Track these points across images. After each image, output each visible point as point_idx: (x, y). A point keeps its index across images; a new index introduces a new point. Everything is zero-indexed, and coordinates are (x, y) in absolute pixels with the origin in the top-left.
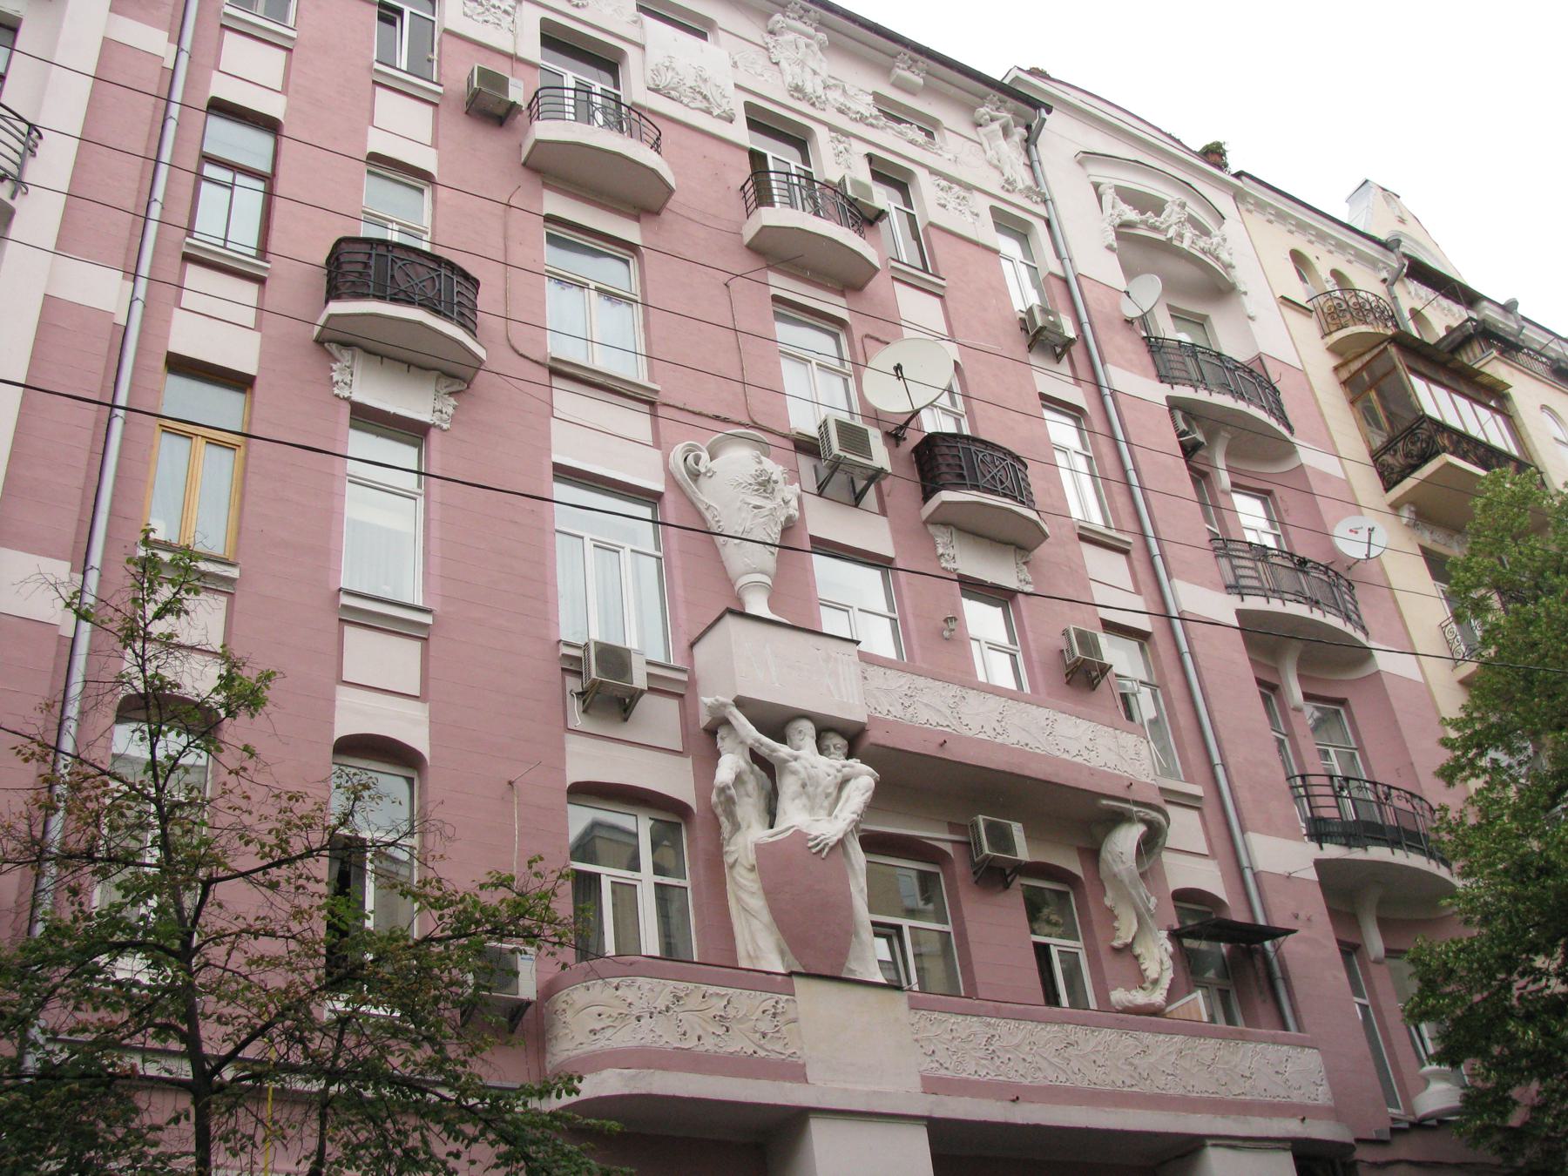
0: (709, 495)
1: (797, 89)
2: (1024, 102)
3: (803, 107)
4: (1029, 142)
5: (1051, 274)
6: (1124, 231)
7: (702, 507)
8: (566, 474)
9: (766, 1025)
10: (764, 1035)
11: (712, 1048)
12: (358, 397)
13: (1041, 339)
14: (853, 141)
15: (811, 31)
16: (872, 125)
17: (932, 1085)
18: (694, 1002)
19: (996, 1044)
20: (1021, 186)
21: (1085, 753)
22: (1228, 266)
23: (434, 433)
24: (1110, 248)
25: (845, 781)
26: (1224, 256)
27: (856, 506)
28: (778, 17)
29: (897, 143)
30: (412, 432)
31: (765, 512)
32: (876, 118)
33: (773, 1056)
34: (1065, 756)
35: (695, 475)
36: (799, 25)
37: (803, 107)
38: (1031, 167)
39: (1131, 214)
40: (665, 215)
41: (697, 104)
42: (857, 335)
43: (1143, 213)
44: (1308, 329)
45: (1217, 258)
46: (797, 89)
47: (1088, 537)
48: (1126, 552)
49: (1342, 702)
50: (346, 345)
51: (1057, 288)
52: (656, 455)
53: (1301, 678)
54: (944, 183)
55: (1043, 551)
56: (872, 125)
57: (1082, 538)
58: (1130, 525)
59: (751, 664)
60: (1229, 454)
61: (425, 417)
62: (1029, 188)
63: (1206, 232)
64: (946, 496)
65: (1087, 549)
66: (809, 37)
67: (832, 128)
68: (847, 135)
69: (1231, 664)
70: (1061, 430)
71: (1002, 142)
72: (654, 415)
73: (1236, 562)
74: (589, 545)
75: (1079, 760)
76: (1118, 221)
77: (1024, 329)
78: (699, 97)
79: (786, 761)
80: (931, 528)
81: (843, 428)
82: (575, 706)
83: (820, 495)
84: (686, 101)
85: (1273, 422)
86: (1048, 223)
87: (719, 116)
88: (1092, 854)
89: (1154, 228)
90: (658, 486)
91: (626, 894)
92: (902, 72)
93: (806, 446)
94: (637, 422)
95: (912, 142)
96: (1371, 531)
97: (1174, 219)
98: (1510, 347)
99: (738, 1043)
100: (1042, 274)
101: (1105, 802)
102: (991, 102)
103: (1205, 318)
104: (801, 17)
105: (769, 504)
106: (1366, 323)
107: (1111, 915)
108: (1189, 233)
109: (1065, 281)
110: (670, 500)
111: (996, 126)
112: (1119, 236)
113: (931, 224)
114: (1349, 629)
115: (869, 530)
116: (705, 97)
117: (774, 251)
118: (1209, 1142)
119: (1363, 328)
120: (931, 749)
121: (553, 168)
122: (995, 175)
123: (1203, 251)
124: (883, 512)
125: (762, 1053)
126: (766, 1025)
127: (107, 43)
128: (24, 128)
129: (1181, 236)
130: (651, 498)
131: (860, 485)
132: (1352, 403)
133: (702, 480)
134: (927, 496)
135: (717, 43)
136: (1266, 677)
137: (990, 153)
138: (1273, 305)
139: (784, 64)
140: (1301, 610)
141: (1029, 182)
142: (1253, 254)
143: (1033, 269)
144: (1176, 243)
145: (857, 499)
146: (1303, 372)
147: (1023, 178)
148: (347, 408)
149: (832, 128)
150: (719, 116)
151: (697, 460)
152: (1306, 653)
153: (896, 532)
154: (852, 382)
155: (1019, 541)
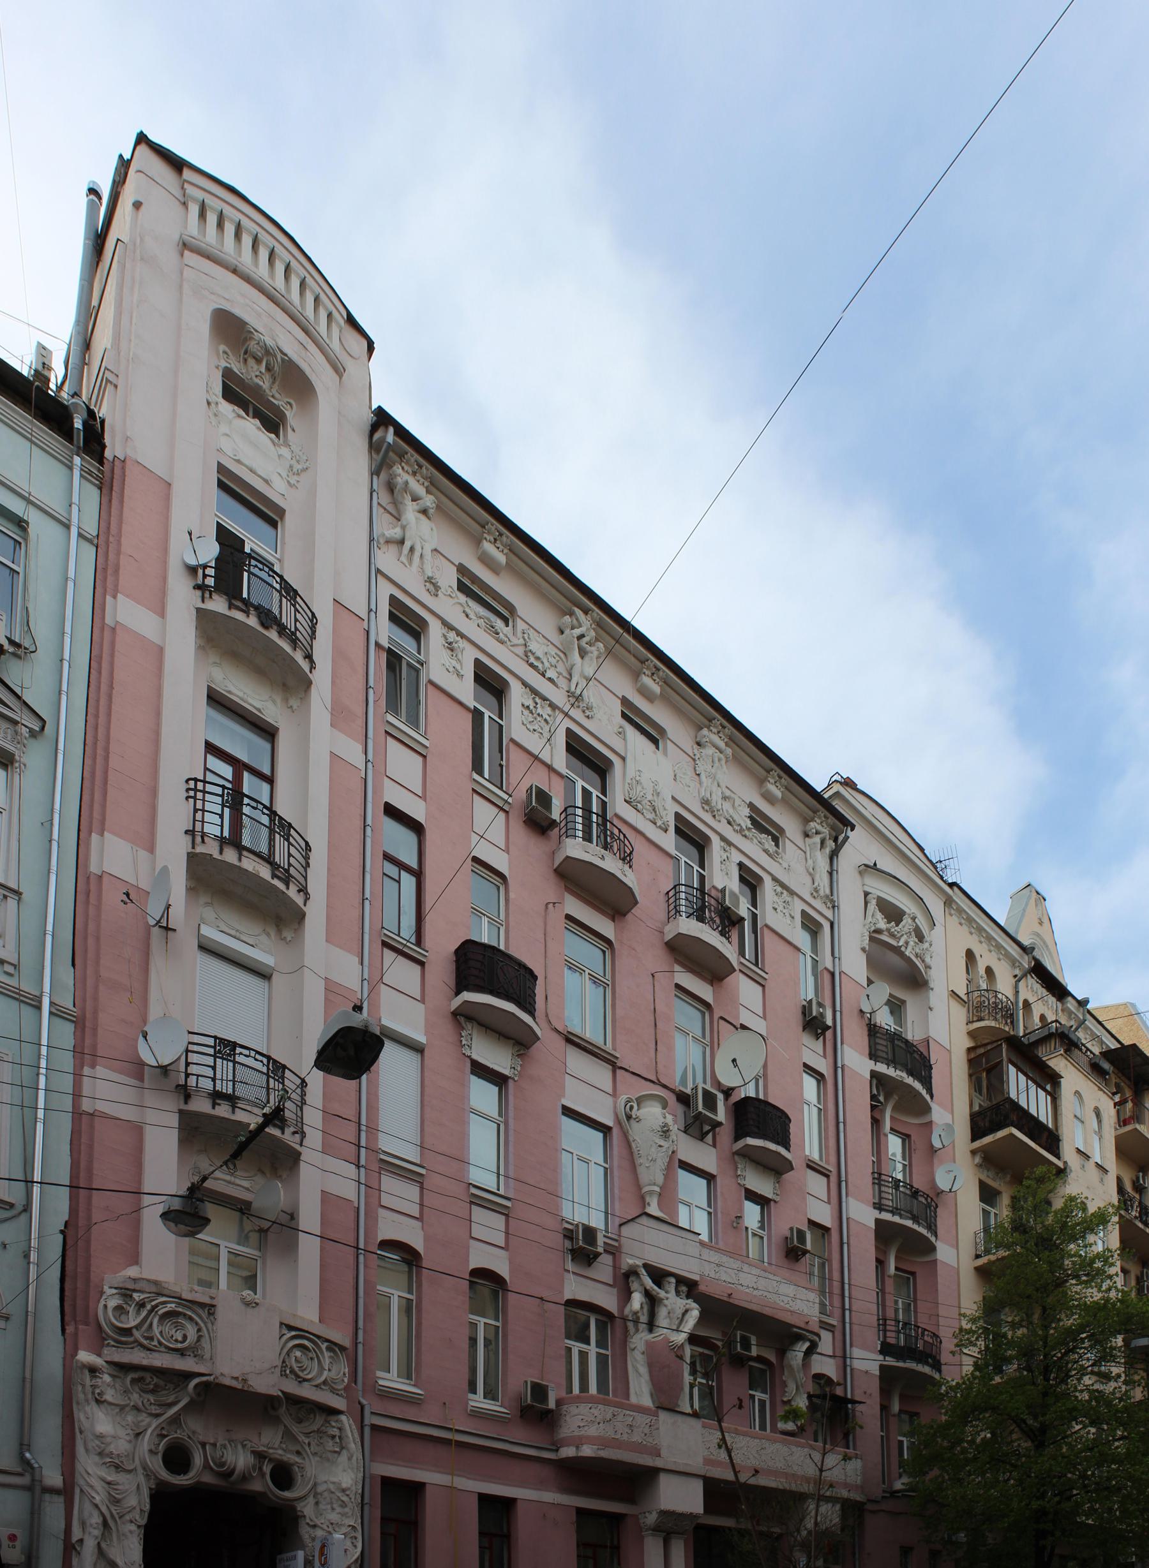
0: (637, 1132)
2: (831, 812)
4: (834, 855)
5: (826, 969)
6: (874, 936)
7: (631, 1139)
8: (568, 1112)
13: (814, 1025)
14: (733, 850)
20: (822, 893)
22: (928, 967)
23: (510, 1081)
24: (863, 950)
26: (928, 960)
32: (749, 829)
35: (629, 1117)
38: (831, 874)
39: (882, 924)
40: (629, 916)
42: (716, 1017)
43: (889, 922)
44: (960, 1014)
45: (923, 961)
46: (706, 802)
47: (811, 1166)
48: (827, 1176)
49: (913, 1274)
51: (827, 977)
52: (610, 1100)
53: (896, 1258)
54: (779, 889)
55: (788, 1176)
56: (745, 836)
57: (809, 1166)
58: (833, 1159)
59: (647, 1245)
61: (506, 1072)
62: (827, 896)
63: (921, 938)
64: (751, 1141)
65: (809, 1171)
67: (723, 839)
68: (730, 844)
69: (864, 1250)
70: (809, 1085)
71: (818, 853)
72: (614, 1072)
73: (883, 1189)
74: (575, 1158)
77: (804, 1013)
80: (736, 1157)
81: (706, 1093)
83: (685, 1132)
85: (924, 1092)
86: (832, 924)
89: (892, 935)
90: (609, 1122)
93: (684, 1099)
94: (601, 1075)
96: (958, 1175)
97: (906, 930)
98: (1068, 1042)
100: (820, 968)
103: (903, 1002)
106: (995, 1019)
108: (913, 940)
109: (833, 974)
110: (616, 1132)
112: (871, 939)
113: (767, 926)
114: (929, 1235)
115: (705, 1156)
119: (993, 1024)
122: (808, 880)
124: (714, 1145)
129: (907, 943)
130: (605, 1130)
131: (707, 1128)
132: (970, 1076)
133: (632, 1121)
134: (737, 1138)
135: (665, 753)
136: (881, 1258)
137: (810, 862)
138: (946, 994)
140: (909, 1223)
141: (828, 892)
142: (944, 955)
143: (815, 962)
144: (903, 949)
145: (702, 1137)
146: (949, 1051)
147: (823, 881)
149: (723, 839)
151: (631, 1108)
152: (906, 1243)
153: (719, 1158)
154: (708, 1050)
155: (777, 1168)
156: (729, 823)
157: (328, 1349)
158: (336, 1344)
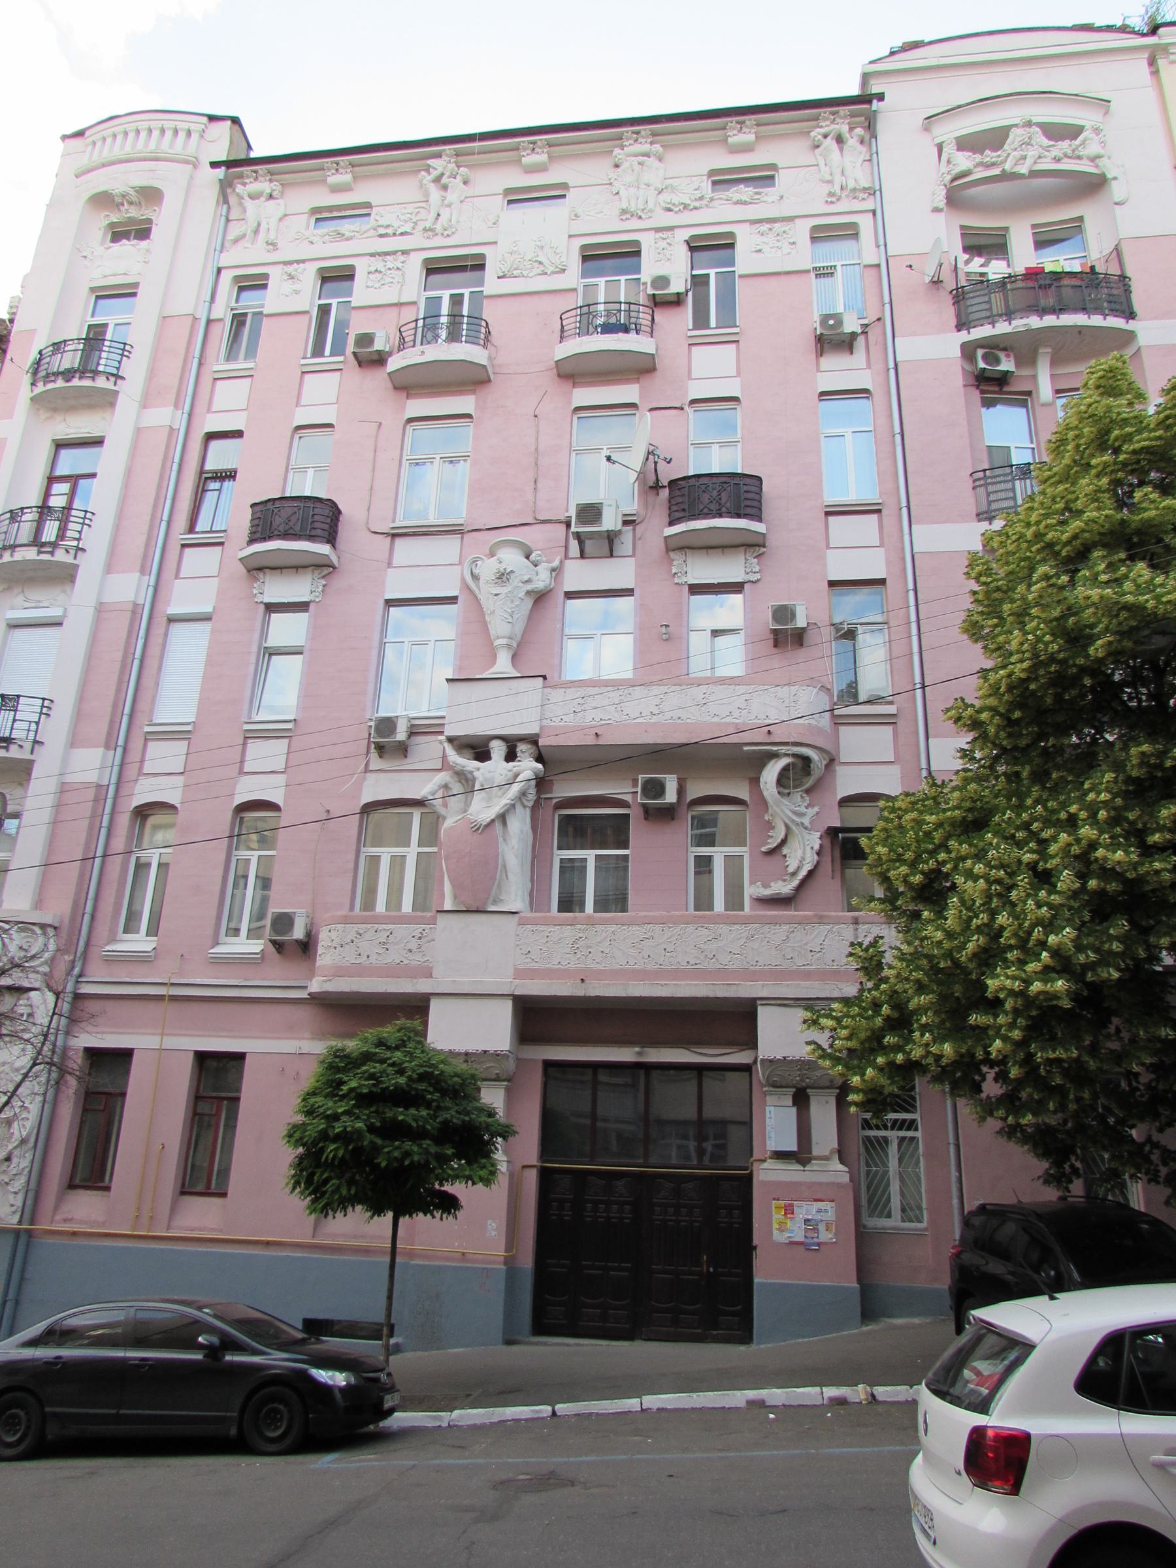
1: (624, 212)
3: (634, 224)
9: (413, 944)
10: (410, 951)
11: (374, 962)
12: (266, 600)
15: (646, 148)
16: (696, 208)
17: (520, 973)
18: (367, 936)
19: (581, 943)
21: (736, 714)
25: (516, 776)
27: (612, 556)
28: (617, 151)
29: (721, 212)
30: (302, 607)
31: (502, 596)
33: (413, 963)
34: (716, 719)
36: (637, 148)
37: (634, 224)
41: (536, 271)
50: (260, 569)
54: (764, 227)
56: (696, 208)
60: (1054, 363)
66: (647, 155)
75: (729, 720)
76: (949, 178)
78: (536, 265)
79: (471, 772)
82: (374, 755)
84: (525, 273)
87: (553, 273)
88: (755, 781)
91: (398, 863)
92: (736, 138)
95: (739, 202)
99: (394, 956)
101: (746, 748)
102: (825, 119)
104: (636, 141)
105: (503, 590)
107: (770, 826)
111: (830, 143)
116: (540, 263)
117: (572, 373)
118: (759, 1002)
120: (590, 740)
121: (409, 384)
123: (1057, 160)
125: (406, 962)
126: (413, 944)
127: (138, 431)
128: (82, 514)
139: (623, 193)
148: (262, 606)
150: (553, 273)
156: (669, 210)
157: (21, 930)
158: (34, 924)
